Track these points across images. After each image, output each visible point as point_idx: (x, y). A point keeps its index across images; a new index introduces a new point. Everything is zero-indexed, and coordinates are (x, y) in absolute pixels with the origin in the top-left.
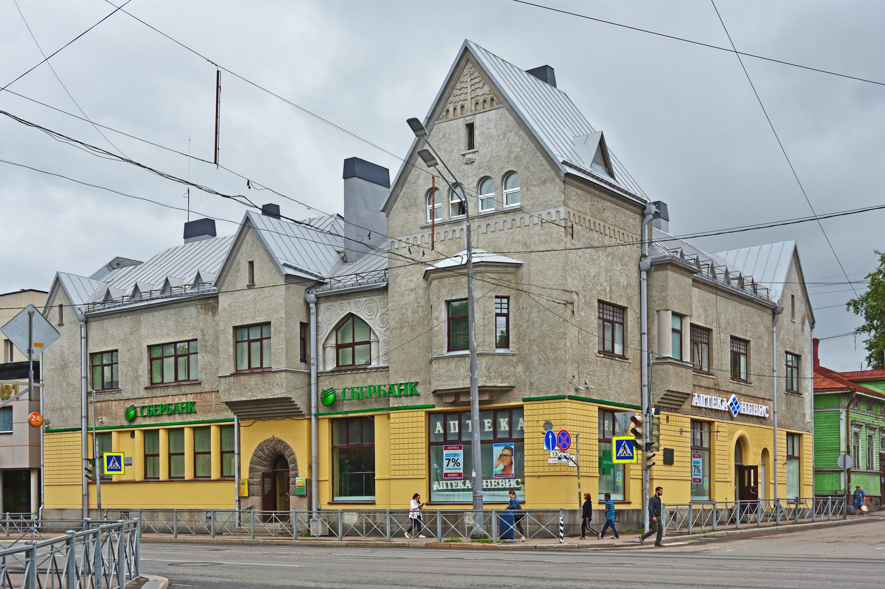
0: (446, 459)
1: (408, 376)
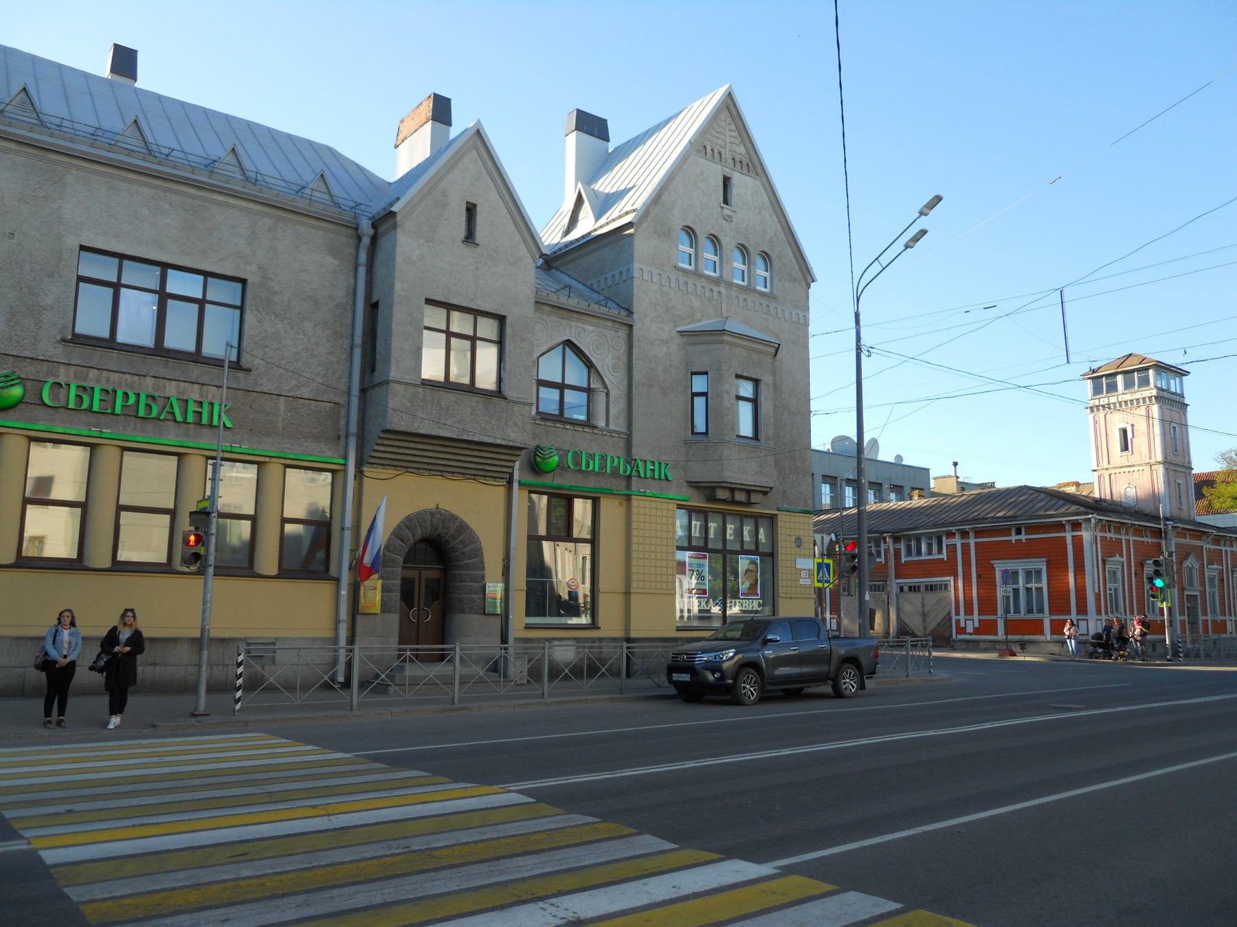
0: (690, 570)
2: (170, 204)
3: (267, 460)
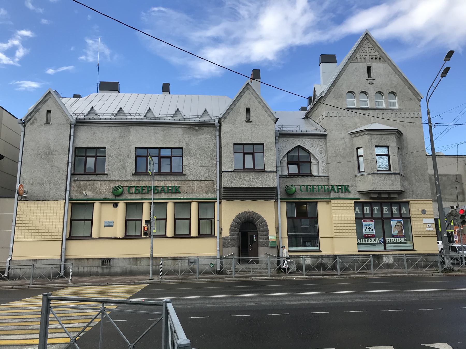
0: (364, 227)
1: (342, 182)
2: (159, 130)
3: (192, 201)
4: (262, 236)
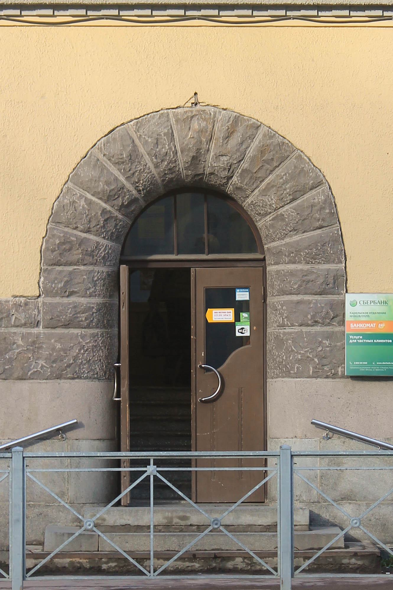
4: (295, 298)
